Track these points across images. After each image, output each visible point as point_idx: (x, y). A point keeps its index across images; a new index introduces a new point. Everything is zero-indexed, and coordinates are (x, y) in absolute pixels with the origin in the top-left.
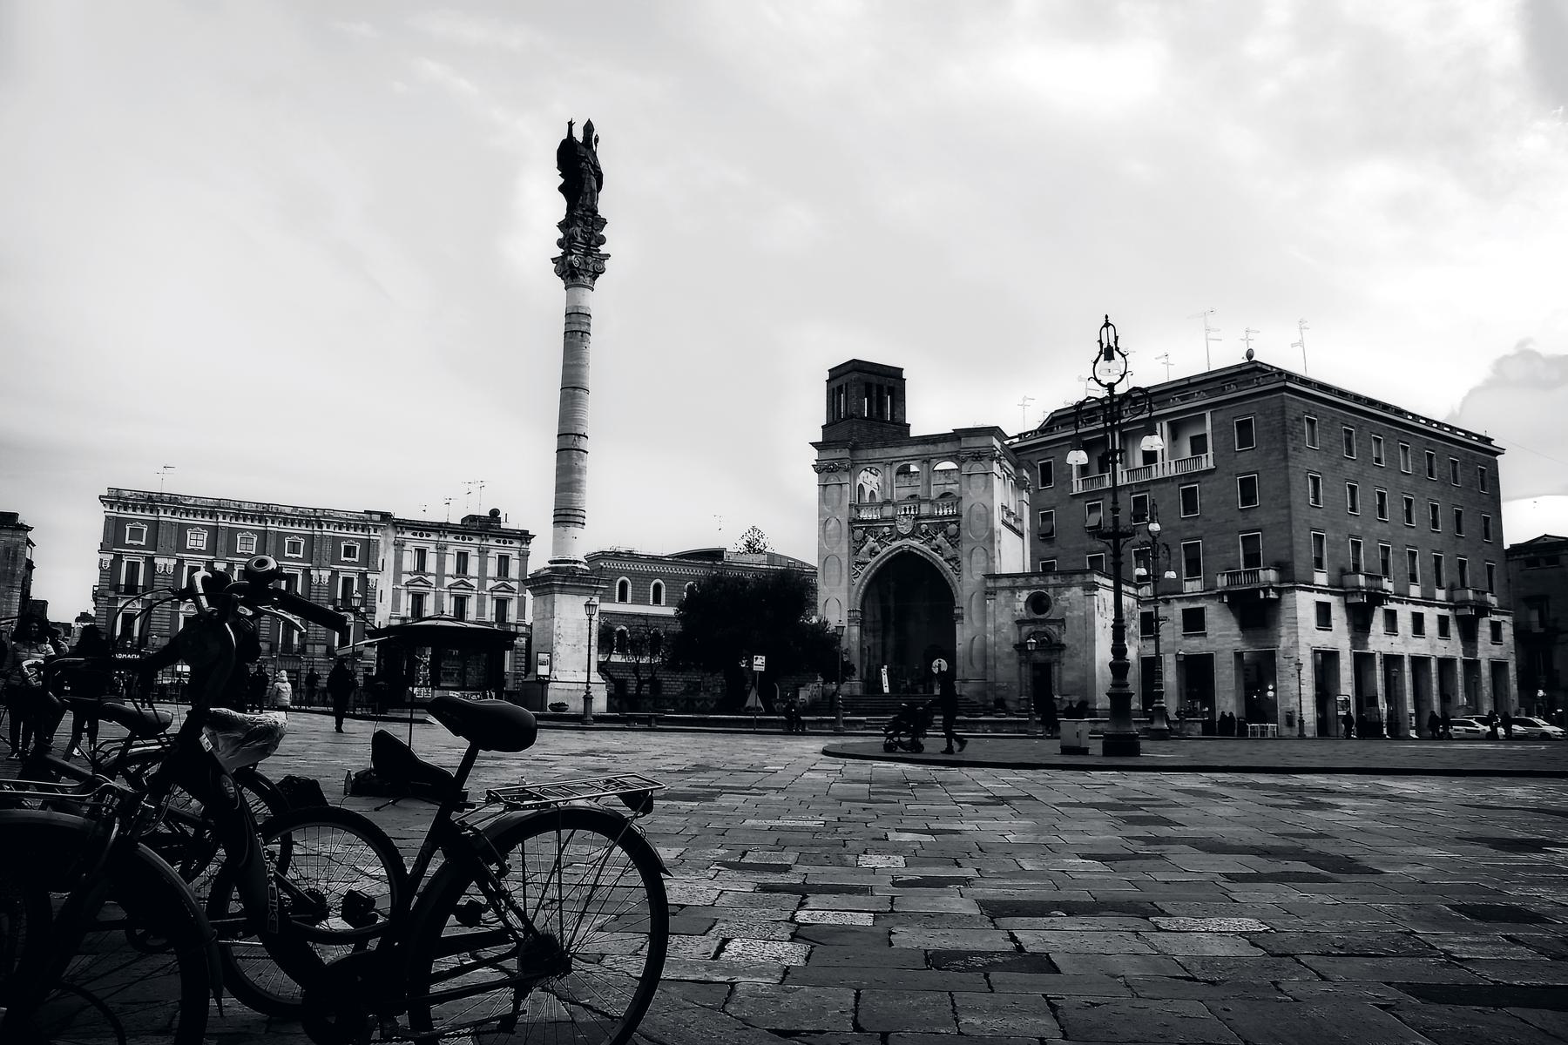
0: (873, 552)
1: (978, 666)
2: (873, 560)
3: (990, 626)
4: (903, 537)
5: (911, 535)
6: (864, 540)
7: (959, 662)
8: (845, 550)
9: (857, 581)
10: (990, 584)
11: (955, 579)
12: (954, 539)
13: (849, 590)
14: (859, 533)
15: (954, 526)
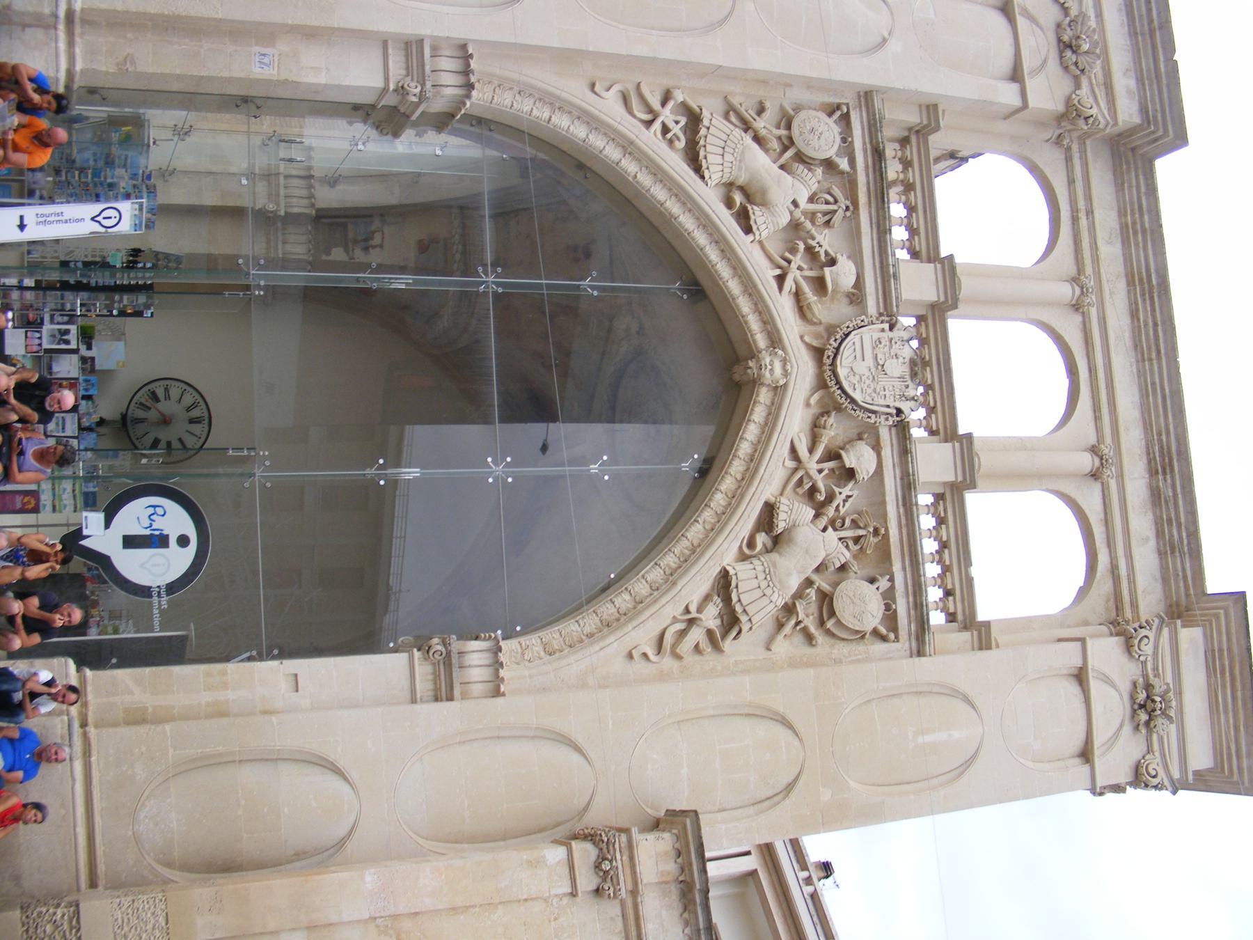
0: (744, 201)
1: (168, 817)
2: (709, 197)
3: (427, 882)
4: (824, 356)
5: (831, 395)
6: (793, 155)
7: (187, 683)
8: (759, 60)
9: (609, 107)
10: (653, 855)
11: (641, 635)
12: (816, 612)
13: (567, 58)
14: (822, 138)
15: (873, 616)
